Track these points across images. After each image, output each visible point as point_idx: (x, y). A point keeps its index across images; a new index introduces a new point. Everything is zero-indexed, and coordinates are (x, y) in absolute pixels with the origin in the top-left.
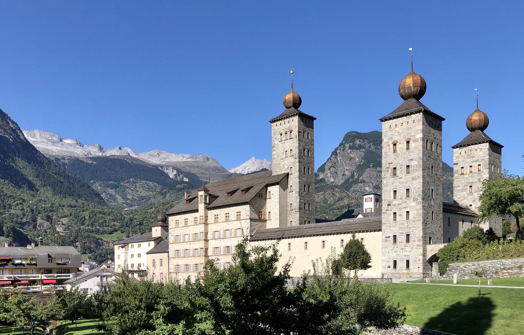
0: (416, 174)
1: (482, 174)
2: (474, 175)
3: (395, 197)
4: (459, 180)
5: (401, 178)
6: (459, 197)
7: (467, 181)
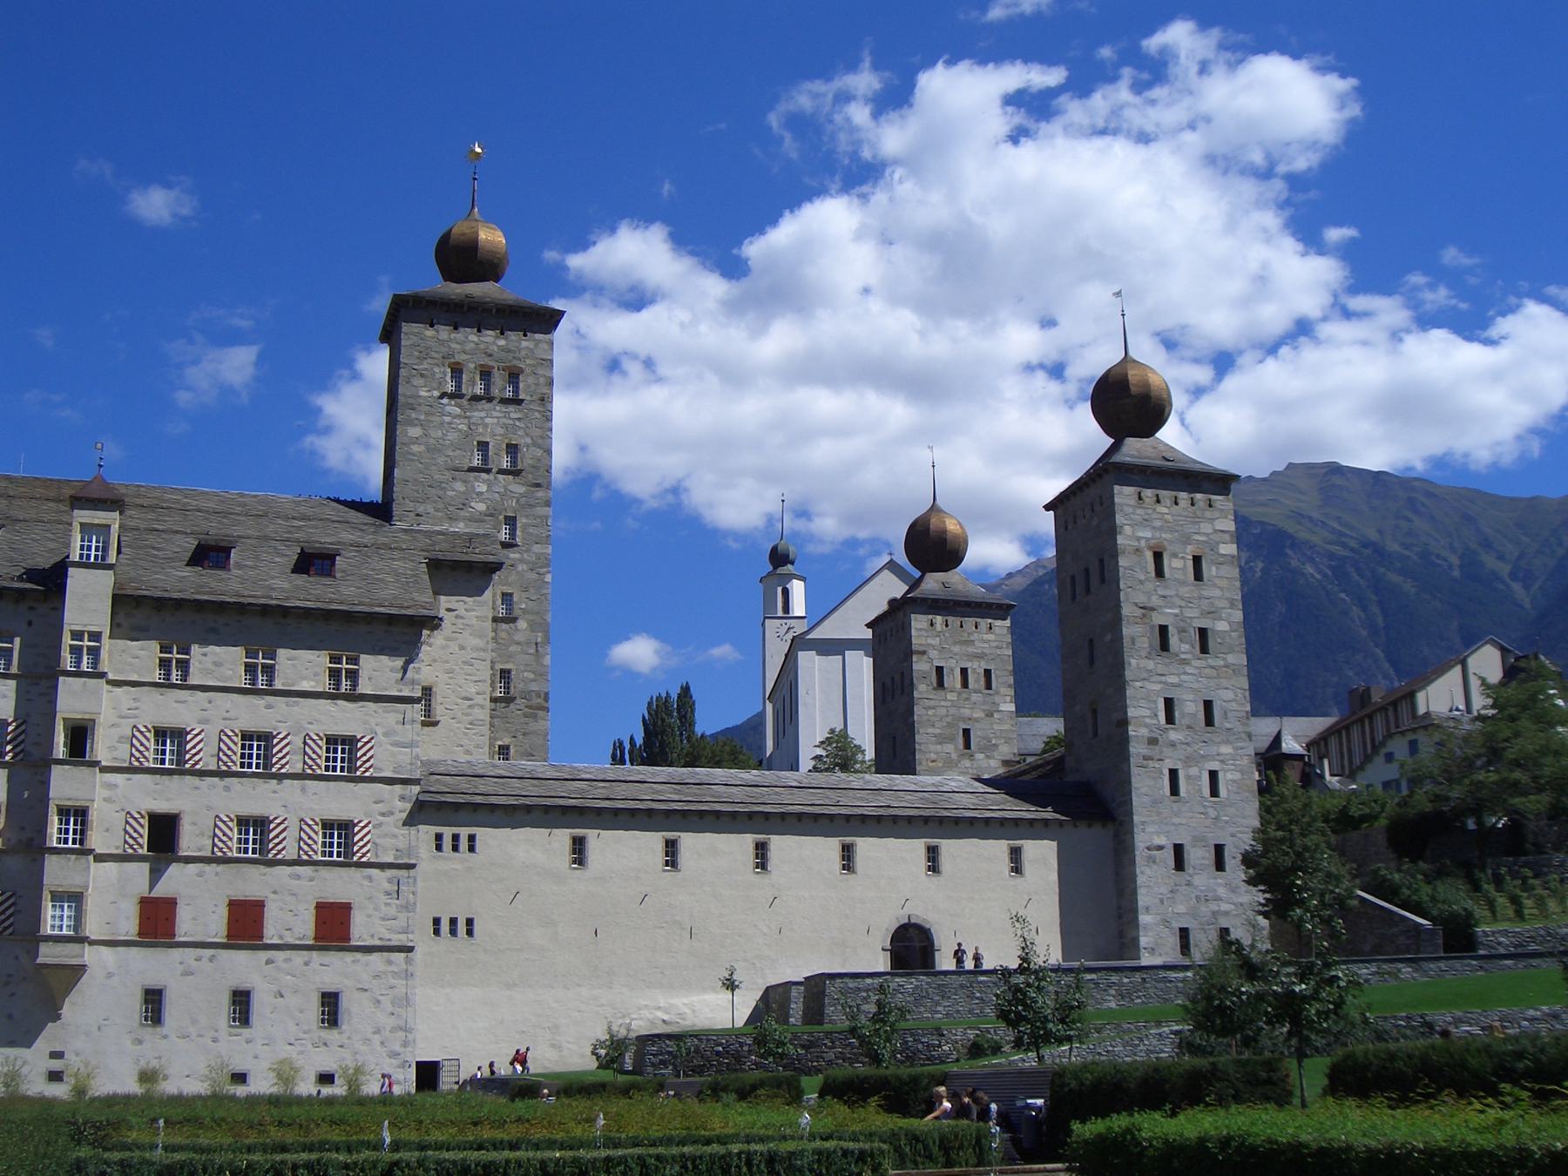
0: (1231, 659)
1: (997, 699)
2: (975, 697)
3: (1170, 719)
4: (932, 703)
5: (1185, 662)
6: (933, 756)
7: (952, 711)
